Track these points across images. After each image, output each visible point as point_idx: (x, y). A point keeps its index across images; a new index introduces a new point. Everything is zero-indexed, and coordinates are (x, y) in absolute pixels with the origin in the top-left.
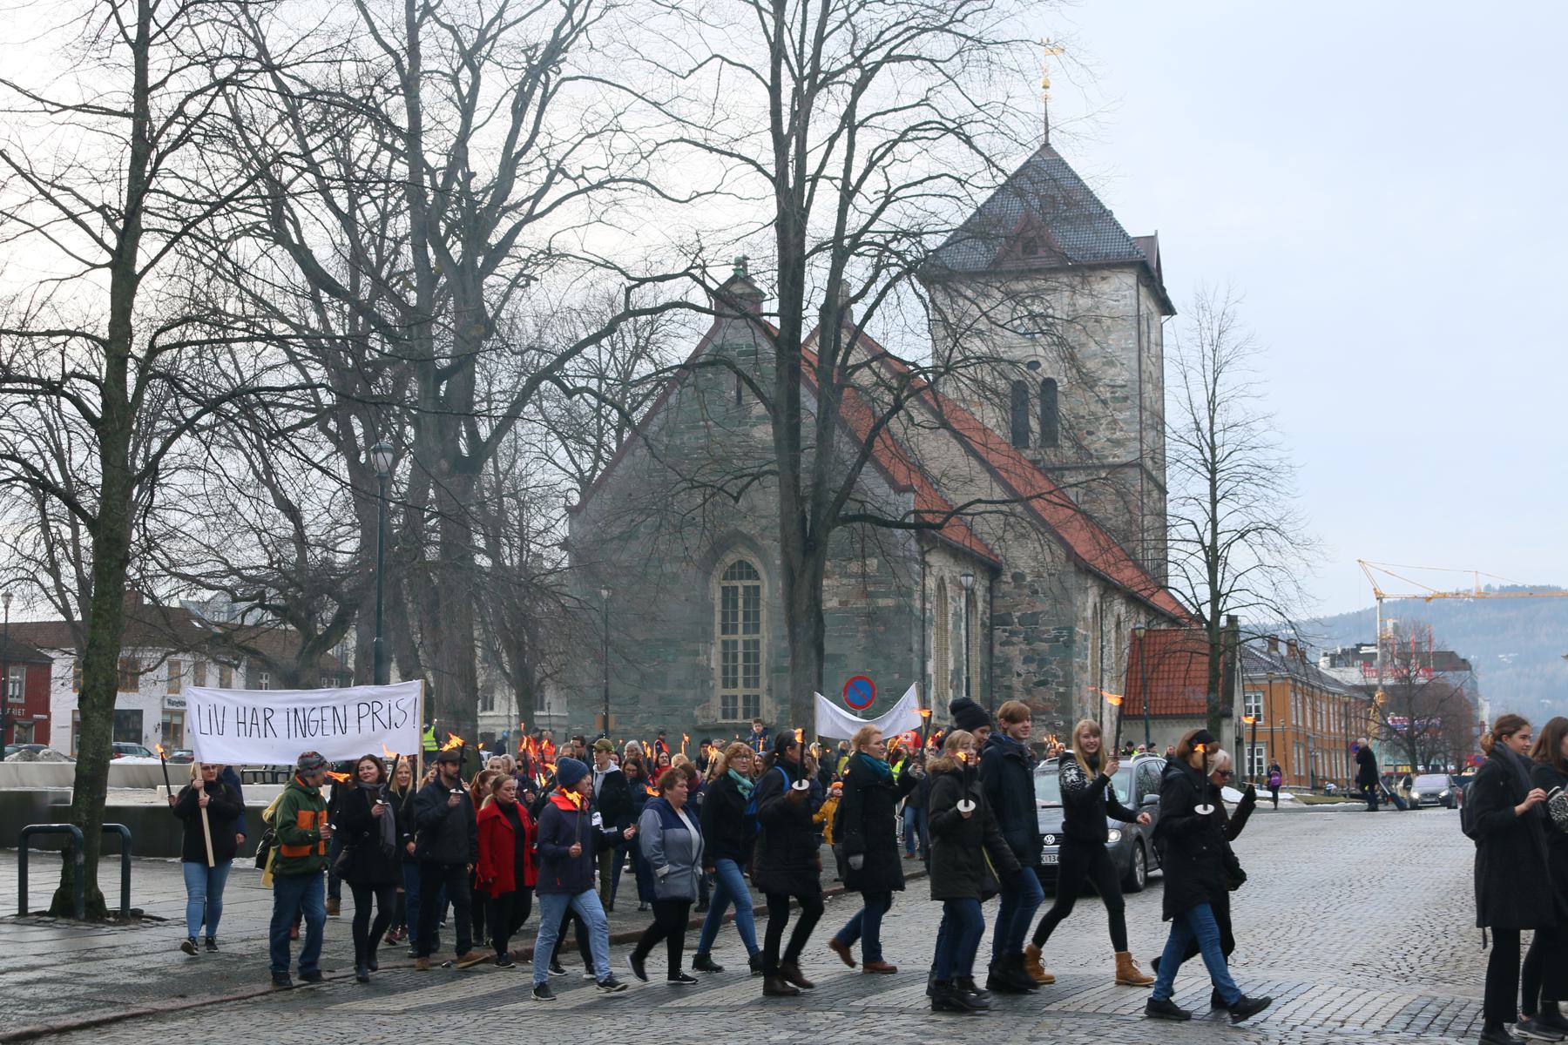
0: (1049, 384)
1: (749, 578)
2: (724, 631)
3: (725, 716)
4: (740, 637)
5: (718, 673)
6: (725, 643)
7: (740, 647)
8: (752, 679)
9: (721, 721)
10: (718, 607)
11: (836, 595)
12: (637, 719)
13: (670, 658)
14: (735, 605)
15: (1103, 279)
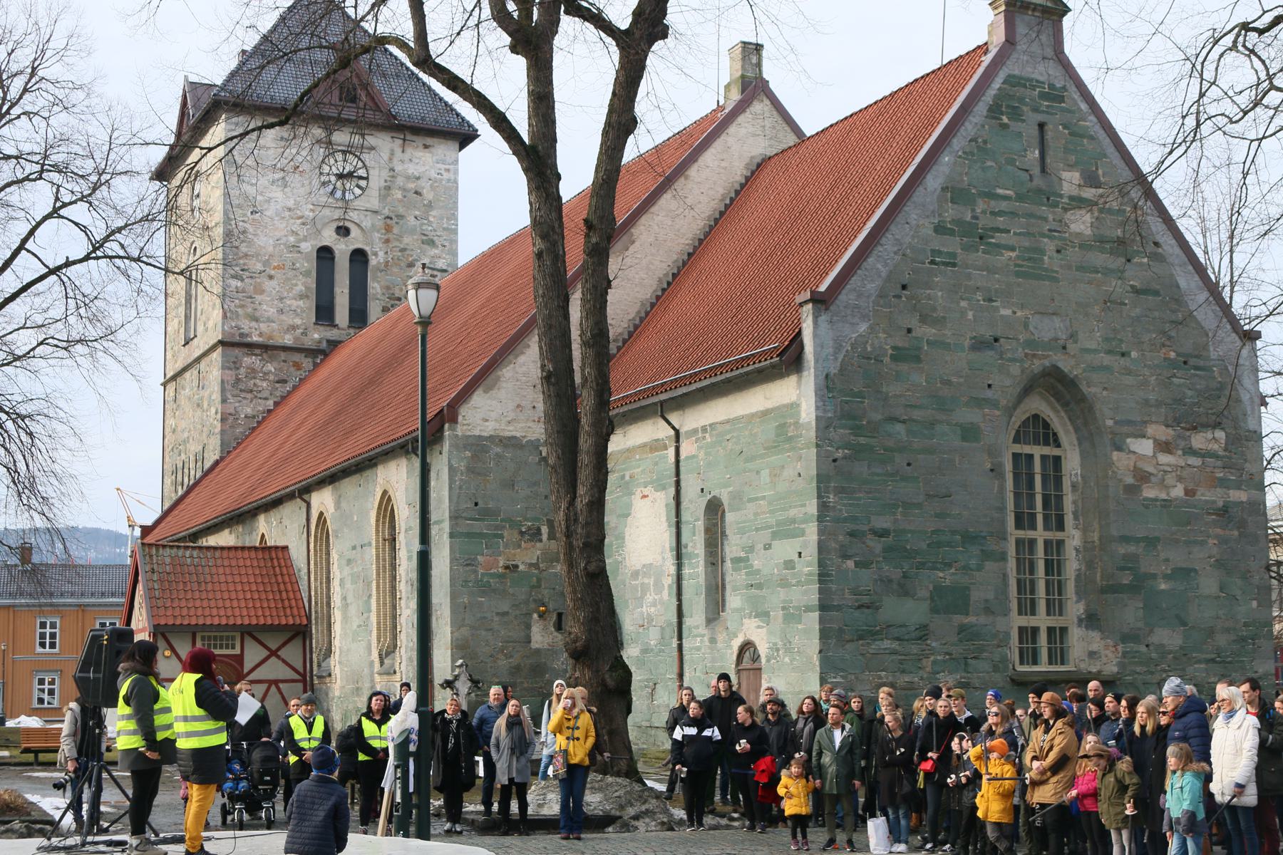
0: (359, 257)
1: (1047, 443)
4: (1040, 534)
8: (1055, 607)
11: (1180, 479)
12: (927, 663)
15: (426, 147)
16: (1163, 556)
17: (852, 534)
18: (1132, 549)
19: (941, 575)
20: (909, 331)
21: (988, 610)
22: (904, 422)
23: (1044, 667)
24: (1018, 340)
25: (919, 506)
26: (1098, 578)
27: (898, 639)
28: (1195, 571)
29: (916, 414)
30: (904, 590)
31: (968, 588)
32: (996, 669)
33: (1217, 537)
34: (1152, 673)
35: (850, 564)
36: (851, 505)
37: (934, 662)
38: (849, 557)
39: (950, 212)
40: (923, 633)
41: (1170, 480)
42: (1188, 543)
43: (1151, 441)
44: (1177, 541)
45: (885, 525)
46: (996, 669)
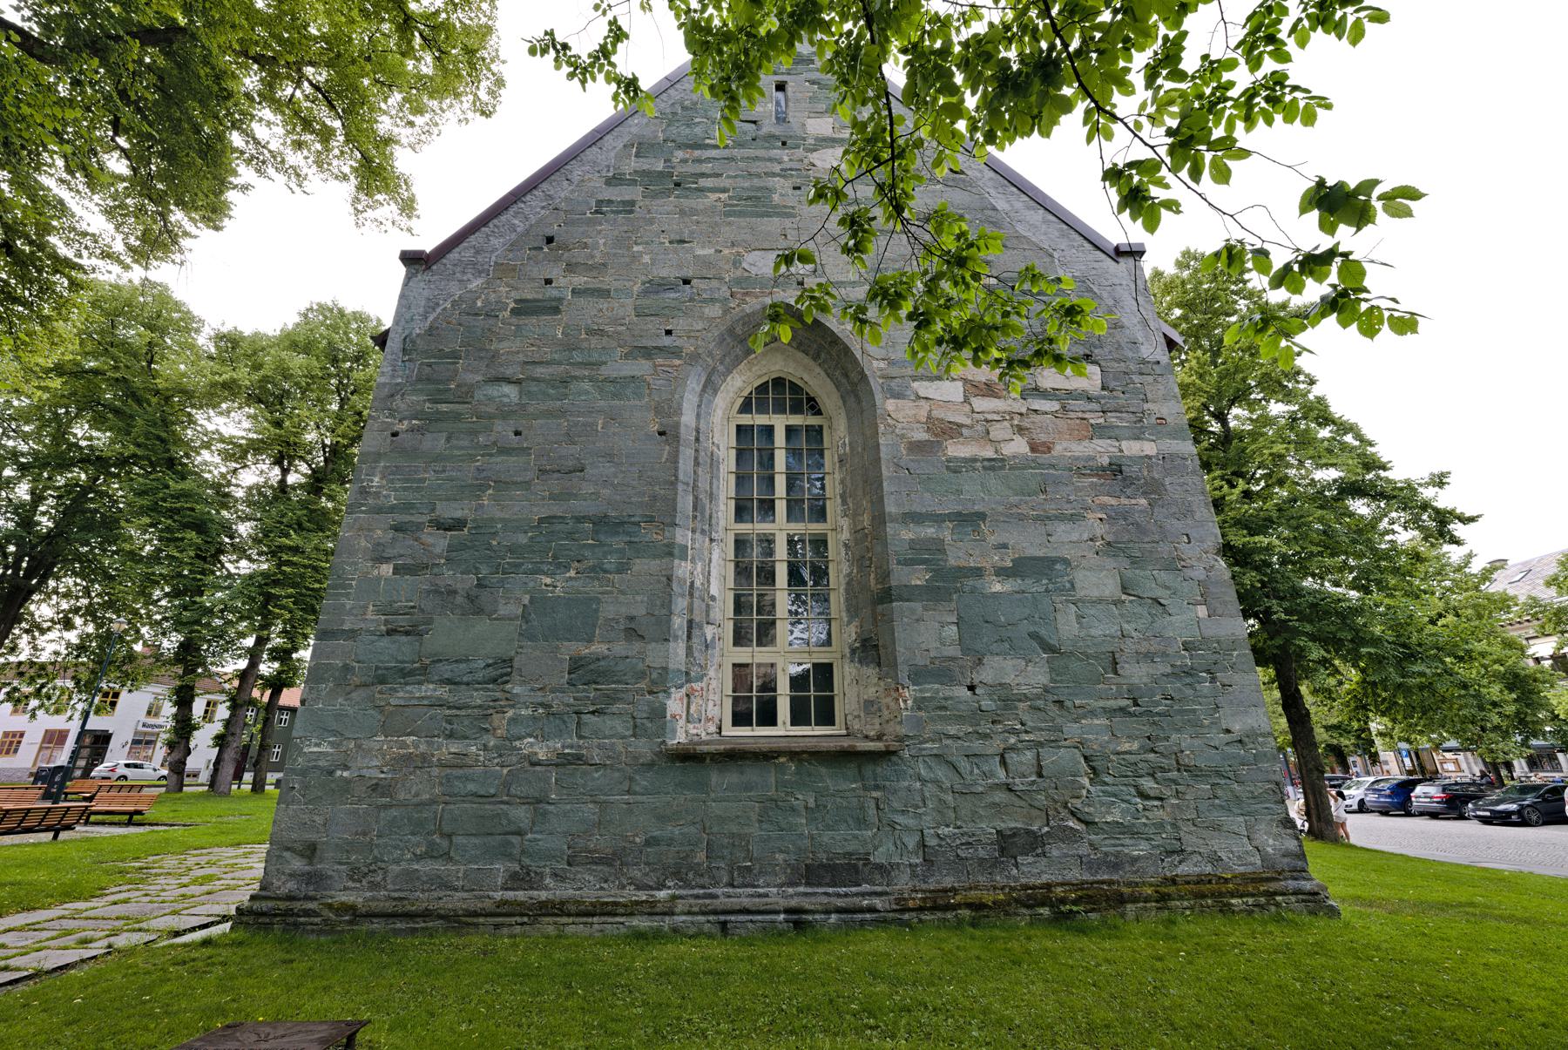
1: (796, 409)
2: (742, 512)
3: (740, 719)
4: (781, 527)
5: (724, 609)
6: (741, 544)
7: (781, 551)
9: (730, 731)
10: (728, 461)
11: (1020, 430)
12: (500, 722)
13: (611, 562)
14: (768, 460)
16: (992, 540)
17: (397, 528)
18: (930, 531)
19: (548, 581)
20: (548, 282)
21: (633, 633)
22: (518, 382)
23: (783, 728)
24: (721, 279)
25: (526, 485)
26: (873, 582)
27: (449, 682)
28: (1066, 562)
29: (540, 371)
30: (475, 606)
31: (599, 601)
32: (637, 731)
33: (1103, 507)
34: (986, 736)
35: (387, 569)
36: (405, 489)
37: (513, 720)
38: (387, 560)
39: (632, 165)
40: (501, 672)
41: (998, 432)
42: (1044, 519)
43: (960, 384)
44: (1022, 518)
45: (458, 514)
46: (637, 731)
